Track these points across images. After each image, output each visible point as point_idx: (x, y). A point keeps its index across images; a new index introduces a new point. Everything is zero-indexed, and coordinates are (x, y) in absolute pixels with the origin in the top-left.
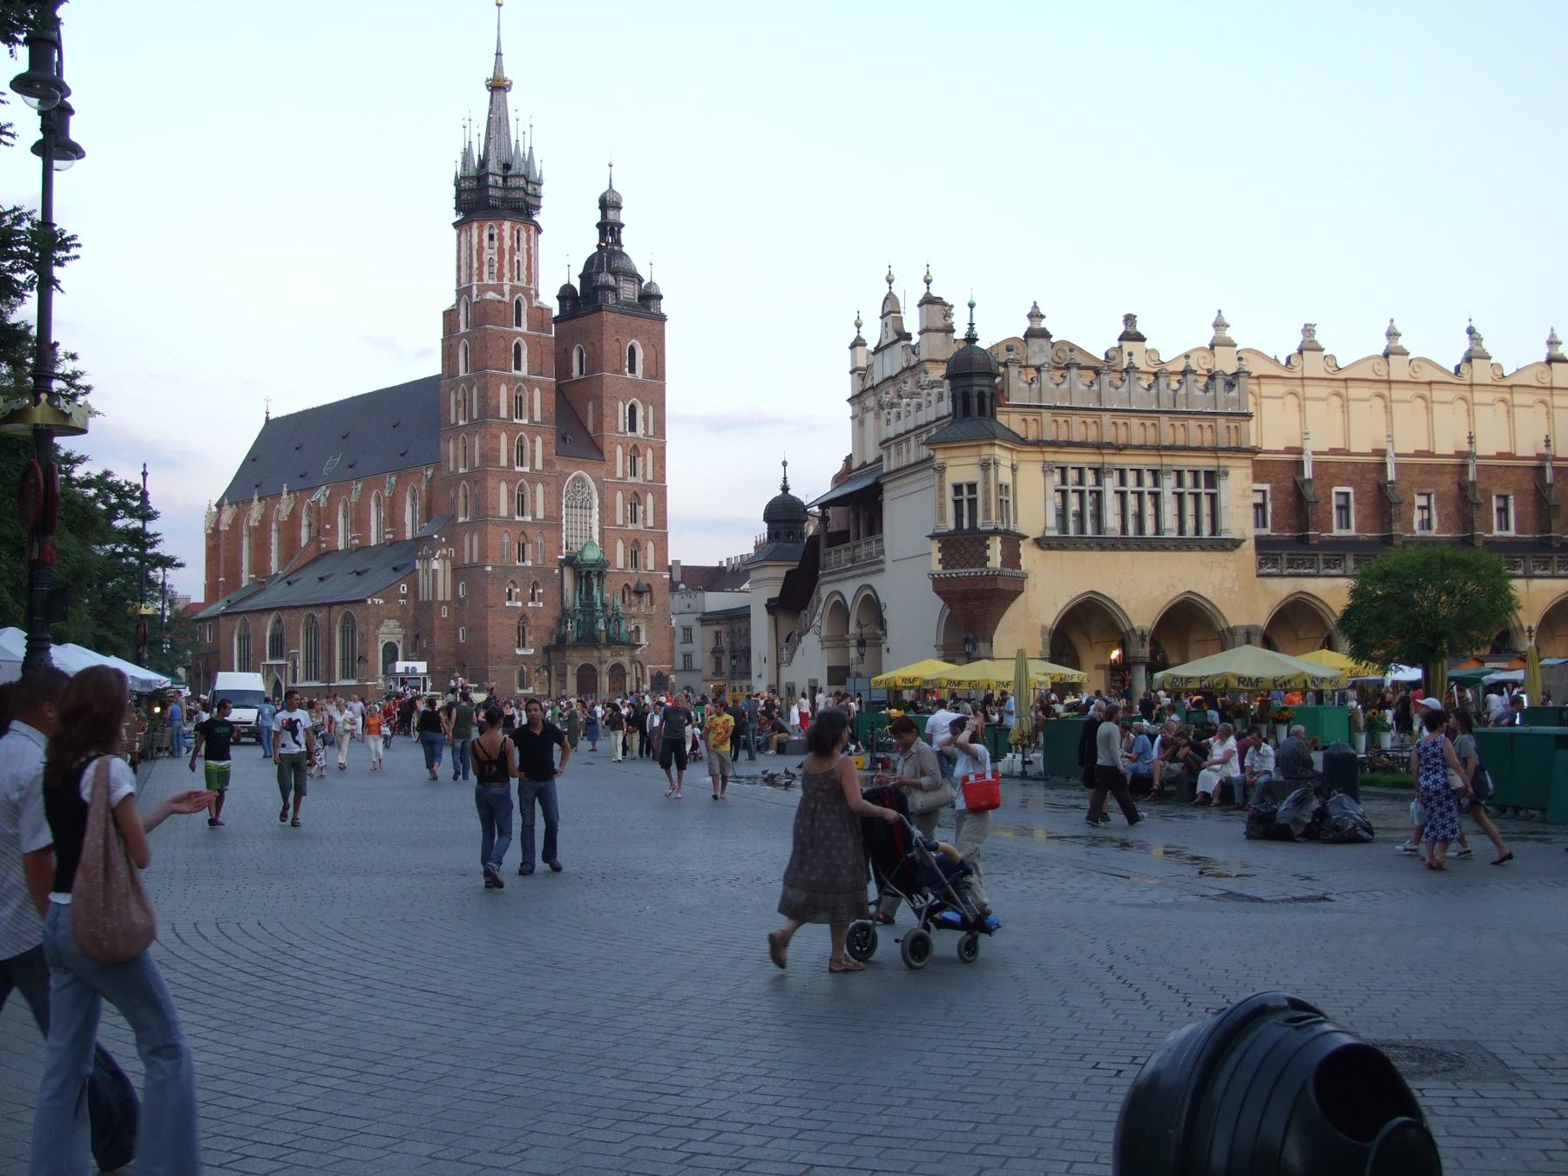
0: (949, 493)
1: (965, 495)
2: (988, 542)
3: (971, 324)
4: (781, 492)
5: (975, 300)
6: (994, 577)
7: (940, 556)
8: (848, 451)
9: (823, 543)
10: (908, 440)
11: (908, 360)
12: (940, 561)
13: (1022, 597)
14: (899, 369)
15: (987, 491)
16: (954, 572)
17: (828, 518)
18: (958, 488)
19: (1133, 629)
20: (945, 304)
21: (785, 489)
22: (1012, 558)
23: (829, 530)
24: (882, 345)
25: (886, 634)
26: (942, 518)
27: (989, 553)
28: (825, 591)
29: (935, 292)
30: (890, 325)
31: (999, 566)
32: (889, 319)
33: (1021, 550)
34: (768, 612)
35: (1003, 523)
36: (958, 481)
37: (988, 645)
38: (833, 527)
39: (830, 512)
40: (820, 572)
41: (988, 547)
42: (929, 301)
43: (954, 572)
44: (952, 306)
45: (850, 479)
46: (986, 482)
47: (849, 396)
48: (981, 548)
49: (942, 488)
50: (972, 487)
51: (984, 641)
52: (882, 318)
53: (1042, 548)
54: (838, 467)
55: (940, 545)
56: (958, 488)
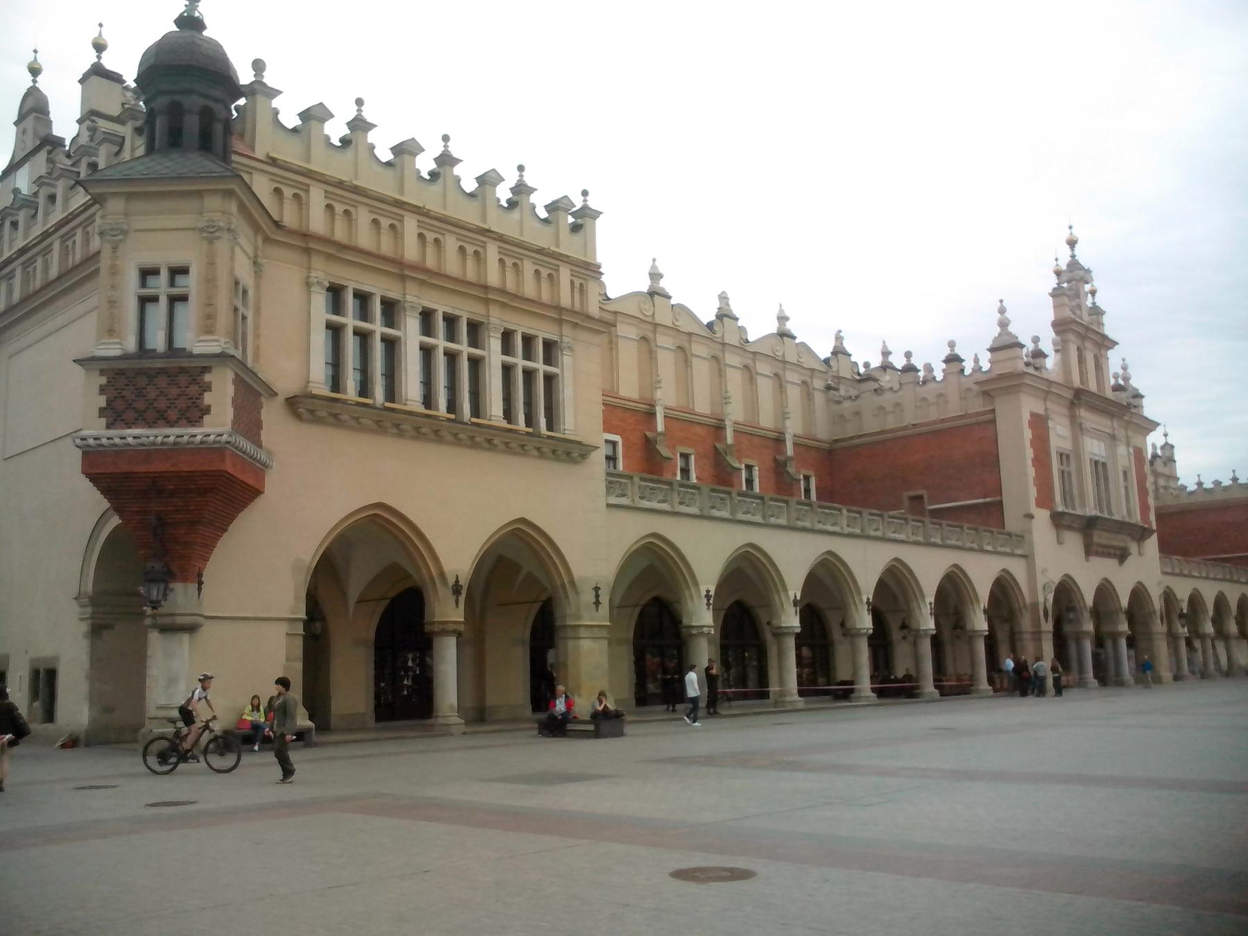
0: (132, 278)
2: (207, 377)
6: (217, 451)
10: (47, 250)
12: (102, 412)
13: (259, 503)
15: (210, 281)
16: (135, 435)
18: (147, 273)
19: (442, 574)
22: (249, 422)
26: (111, 331)
27: (208, 398)
30: (30, 132)
31: (228, 427)
33: (264, 416)
35: (236, 348)
36: (149, 258)
37: (193, 587)
41: (208, 388)
43: (135, 435)
46: (211, 263)
48: (193, 390)
50: (178, 271)
51: (185, 580)
52: (16, 124)
53: (298, 417)
55: (103, 380)
56: (147, 273)
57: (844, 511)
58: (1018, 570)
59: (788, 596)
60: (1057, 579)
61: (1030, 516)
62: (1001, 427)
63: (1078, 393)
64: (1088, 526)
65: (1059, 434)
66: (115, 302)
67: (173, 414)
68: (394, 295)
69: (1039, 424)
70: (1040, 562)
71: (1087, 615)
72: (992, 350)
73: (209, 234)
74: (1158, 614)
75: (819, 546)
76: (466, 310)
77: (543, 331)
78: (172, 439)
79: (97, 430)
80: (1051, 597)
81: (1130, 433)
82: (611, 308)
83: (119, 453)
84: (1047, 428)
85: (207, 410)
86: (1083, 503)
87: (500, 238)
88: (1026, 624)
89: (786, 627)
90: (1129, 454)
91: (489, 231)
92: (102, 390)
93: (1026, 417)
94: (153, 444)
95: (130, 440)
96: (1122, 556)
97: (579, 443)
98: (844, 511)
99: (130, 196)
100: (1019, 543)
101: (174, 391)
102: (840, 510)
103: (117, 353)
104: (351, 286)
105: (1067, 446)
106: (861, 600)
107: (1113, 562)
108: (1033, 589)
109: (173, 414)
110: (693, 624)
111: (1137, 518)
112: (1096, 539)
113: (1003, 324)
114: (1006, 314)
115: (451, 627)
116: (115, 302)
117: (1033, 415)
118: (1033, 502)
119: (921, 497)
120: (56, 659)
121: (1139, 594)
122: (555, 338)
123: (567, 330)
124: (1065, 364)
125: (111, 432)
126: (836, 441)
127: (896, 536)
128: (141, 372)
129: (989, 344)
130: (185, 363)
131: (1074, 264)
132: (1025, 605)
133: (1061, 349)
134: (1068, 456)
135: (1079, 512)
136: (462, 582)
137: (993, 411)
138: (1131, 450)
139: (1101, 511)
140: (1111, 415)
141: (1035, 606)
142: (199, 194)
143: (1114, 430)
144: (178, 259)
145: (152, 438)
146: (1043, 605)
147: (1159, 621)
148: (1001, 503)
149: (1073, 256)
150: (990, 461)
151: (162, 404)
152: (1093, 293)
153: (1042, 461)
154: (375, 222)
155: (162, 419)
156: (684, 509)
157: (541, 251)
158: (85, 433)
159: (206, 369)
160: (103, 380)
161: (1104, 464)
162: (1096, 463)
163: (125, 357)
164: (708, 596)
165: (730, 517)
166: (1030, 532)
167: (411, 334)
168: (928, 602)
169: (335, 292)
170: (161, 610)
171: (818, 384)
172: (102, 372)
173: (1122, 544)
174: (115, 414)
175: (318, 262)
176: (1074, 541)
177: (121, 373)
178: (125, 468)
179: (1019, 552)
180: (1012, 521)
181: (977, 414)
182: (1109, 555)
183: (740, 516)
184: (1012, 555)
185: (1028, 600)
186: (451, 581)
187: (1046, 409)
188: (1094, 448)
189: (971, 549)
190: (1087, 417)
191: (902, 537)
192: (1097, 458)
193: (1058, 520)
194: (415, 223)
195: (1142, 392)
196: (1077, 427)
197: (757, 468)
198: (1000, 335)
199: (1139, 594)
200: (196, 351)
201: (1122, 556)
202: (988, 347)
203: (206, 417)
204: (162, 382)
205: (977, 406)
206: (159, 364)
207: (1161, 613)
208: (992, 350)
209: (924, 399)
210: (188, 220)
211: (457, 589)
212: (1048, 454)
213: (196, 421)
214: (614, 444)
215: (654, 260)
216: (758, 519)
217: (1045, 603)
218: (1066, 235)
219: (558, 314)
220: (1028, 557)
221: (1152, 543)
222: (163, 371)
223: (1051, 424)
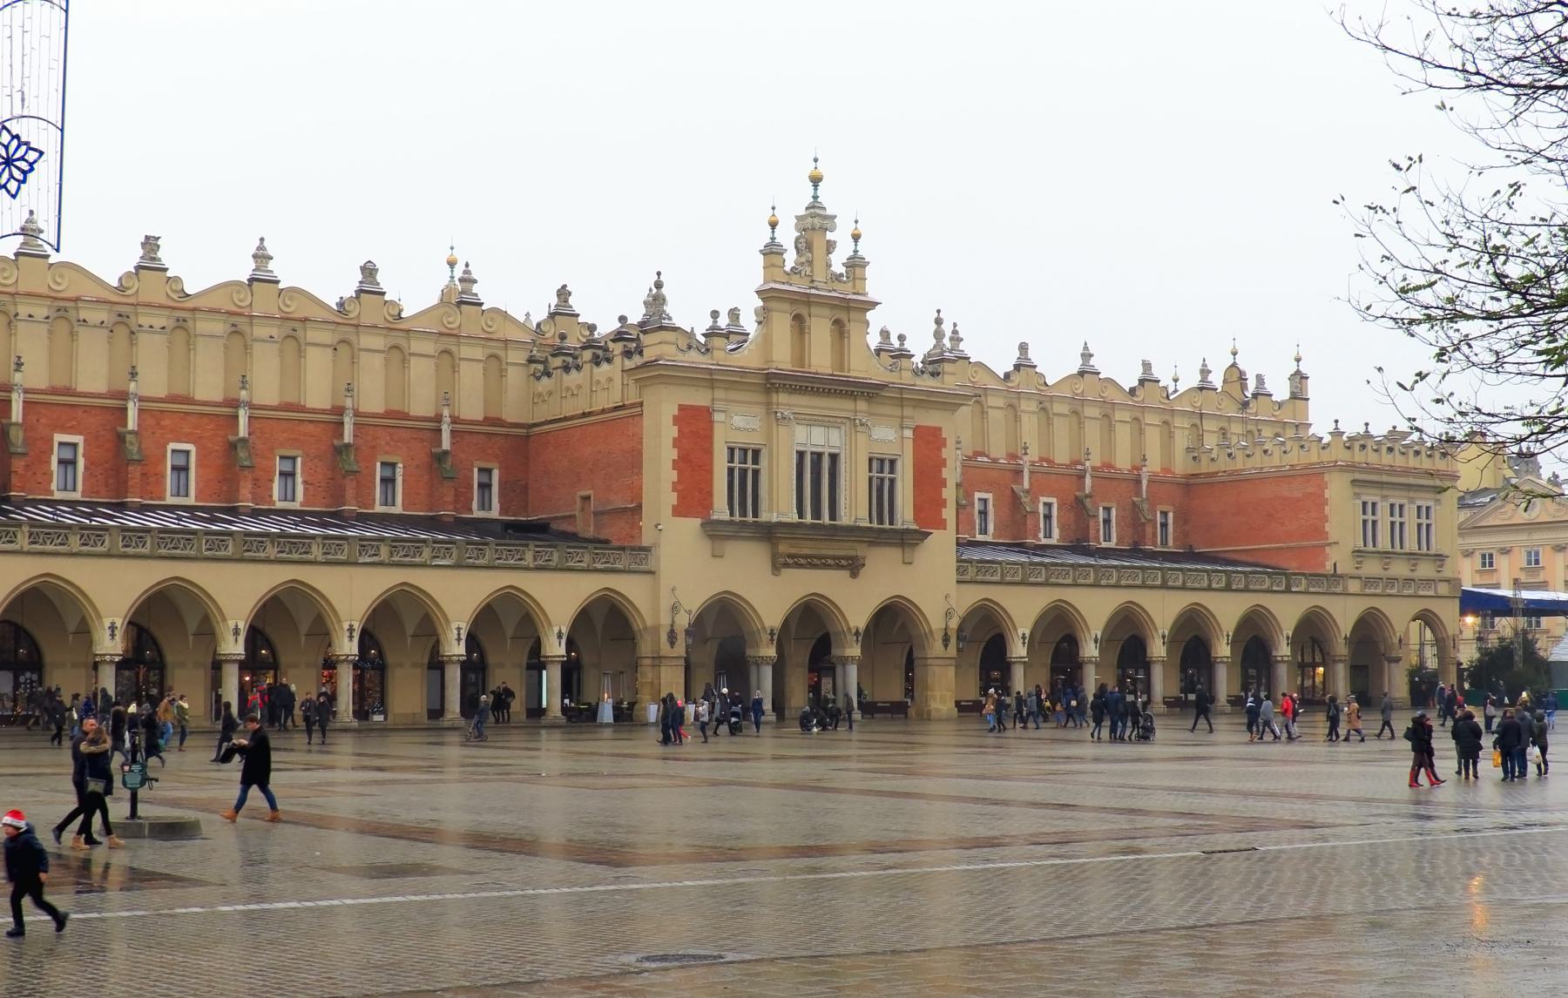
58: (631, 588)
59: (228, 625)
60: (694, 599)
62: (647, 421)
64: (769, 533)
71: (765, 637)
74: (939, 637)
80: (683, 621)
81: (908, 411)
82: (189, 304)
84: (711, 422)
89: (224, 655)
96: (854, 566)
107: (845, 574)
108: (656, 609)
114: (663, 290)
117: (682, 408)
119: (589, 497)
124: (766, 340)
126: (535, 425)
132: (645, 628)
133: (764, 317)
134: (756, 453)
135: (764, 517)
137: (641, 404)
138: (908, 433)
141: (656, 629)
146: (668, 629)
147: (939, 644)
150: (634, 461)
162: (817, 457)
168: (454, 626)
171: (517, 356)
173: (853, 553)
181: (633, 406)
182: (839, 567)
183: (163, 551)
185: (649, 623)
187: (713, 400)
188: (819, 439)
190: (785, 401)
192: (819, 450)
196: (775, 417)
197: (400, 465)
207: (946, 634)
209: (598, 382)
212: (709, 452)
214: (187, 453)
215: (262, 240)
217: (672, 625)
218: (809, 168)
223: (717, 417)
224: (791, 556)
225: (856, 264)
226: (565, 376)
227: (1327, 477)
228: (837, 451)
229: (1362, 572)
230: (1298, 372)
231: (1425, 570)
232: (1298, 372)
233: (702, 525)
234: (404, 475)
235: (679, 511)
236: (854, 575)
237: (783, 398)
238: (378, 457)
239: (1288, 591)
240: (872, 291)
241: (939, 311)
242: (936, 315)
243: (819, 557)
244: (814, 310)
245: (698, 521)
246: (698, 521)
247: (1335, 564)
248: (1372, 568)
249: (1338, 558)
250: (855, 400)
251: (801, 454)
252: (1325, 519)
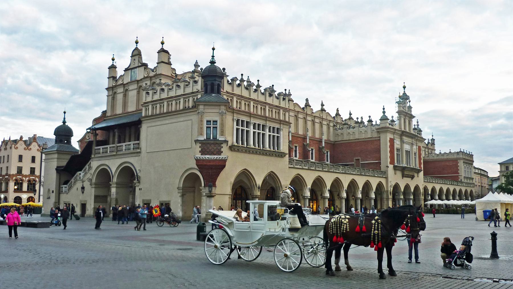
0: (205, 122)
1: (212, 124)
2: (222, 145)
3: (213, 56)
4: (62, 124)
5: (215, 47)
7: (200, 149)
8: (104, 108)
9: (94, 143)
11: (148, 73)
12: (200, 152)
14: (142, 77)
17: (97, 135)
18: (208, 122)
19: (256, 184)
20: (168, 53)
21: (64, 122)
23: (97, 140)
24: (131, 67)
25: (139, 182)
27: (222, 150)
28: (95, 164)
29: (165, 48)
32: (137, 58)
34: (57, 172)
36: (209, 119)
38: (99, 138)
39: (97, 132)
40: (93, 156)
42: (163, 51)
44: (171, 55)
45: (105, 120)
47: (107, 87)
48: (219, 148)
49: (202, 121)
53: (231, 150)
54: (99, 114)
56: (208, 122)
57: (341, 167)
58: (383, 181)
61: (388, 167)
63: (403, 132)
65: (397, 144)
66: (202, 128)
67: (215, 153)
68: (248, 121)
69: (392, 141)
70: (390, 179)
71: (401, 194)
72: (380, 120)
73: (222, 114)
75: (335, 176)
76: (262, 122)
77: (277, 126)
78: (215, 158)
79: (199, 155)
80: (392, 189)
81: (417, 142)
83: (203, 160)
85: (222, 152)
86: (402, 163)
87: (269, 104)
88: (385, 196)
89: (326, 197)
90: (417, 148)
91: (267, 103)
92: (200, 147)
93: (388, 139)
94: (211, 159)
95: (207, 158)
96: (412, 177)
97: (284, 153)
98: (341, 167)
99: (204, 105)
100: (384, 174)
101: (215, 148)
102: (340, 167)
103: (203, 139)
104: (241, 119)
105: (399, 147)
106: (344, 190)
107: (410, 179)
109: (215, 153)
110: (306, 196)
111: (418, 167)
112: (405, 173)
113: (384, 112)
114: (384, 110)
115: (258, 196)
116: (202, 128)
117: (390, 138)
118: (389, 163)
120: (170, 201)
121: (417, 188)
122: (279, 127)
123: (282, 126)
125: (202, 156)
127: (353, 173)
128: (208, 143)
129: (380, 118)
130: (218, 142)
131: (404, 94)
134: (399, 150)
136: (260, 186)
138: (417, 147)
139: (408, 165)
140: (412, 138)
142: (220, 105)
143: (412, 142)
144: (215, 119)
145: (211, 158)
148: (380, 162)
149: (404, 91)
150: (378, 151)
151: (212, 150)
152: (410, 102)
153: (392, 152)
154: (245, 103)
155: (213, 154)
156: (305, 167)
157: (277, 106)
158: (197, 156)
159: (222, 143)
160: (200, 145)
161: (409, 151)
162: (407, 151)
163: (204, 140)
164: (309, 189)
165: (315, 169)
166: (387, 171)
167: (251, 130)
168: (360, 190)
169: (238, 121)
170: (211, 193)
172: (200, 143)
173: (413, 174)
174: (203, 152)
175: (235, 115)
176: (399, 174)
177: (204, 143)
178: (205, 163)
179: (384, 176)
180: (383, 168)
183: (317, 169)
184: (382, 177)
185: (386, 189)
186: (258, 186)
187: (394, 137)
188: (407, 147)
189: (372, 176)
190: (405, 139)
191: (355, 173)
192: (407, 150)
193: (395, 168)
194: (253, 103)
195: (422, 130)
196: (402, 142)
198: (383, 115)
199: (417, 188)
200: (220, 139)
201: (412, 177)
202: (380, 119)
203: (222, 153)
204: (213, 146)
205: (375, 135)
206: (212, 142)
208: (380, 120)
210: (217, 111)
211: (259, 188)
213: (220, 155)
216: (321, 169)
219: (280, 122)
220: (387, 178)
221: (422, 174)
222: (213, 144)
224: (406, 174)
225: (410, 108)
226: (348, 130)
227: (459, 161)
228: (409, 150)
229: (465, 181)
230: (433, 139)
231: (471, 182)
232: (433, 139)
233: (393, 167)
234: (315, 152)
235: (390, 164)
236: (412, 179)
237: (404, 138)
238: (311, 147)
239: (458, 185)
240: (413, 113)
241: (417, 120)
242: (417, 121)
243: (409, 175)
244: (406, 118)
245: (393, 166)
246: (393, 166)
247: (461, 180)
248: (466, 181)
249: (462, 178)
250: (412, 139)
251: (405, 150)
252: (458, 170)
